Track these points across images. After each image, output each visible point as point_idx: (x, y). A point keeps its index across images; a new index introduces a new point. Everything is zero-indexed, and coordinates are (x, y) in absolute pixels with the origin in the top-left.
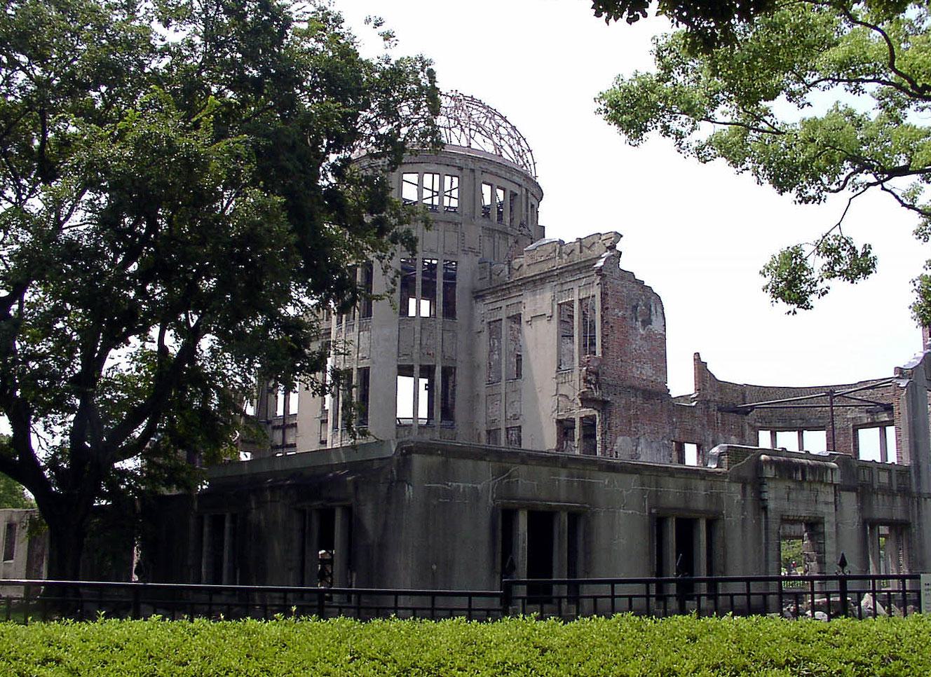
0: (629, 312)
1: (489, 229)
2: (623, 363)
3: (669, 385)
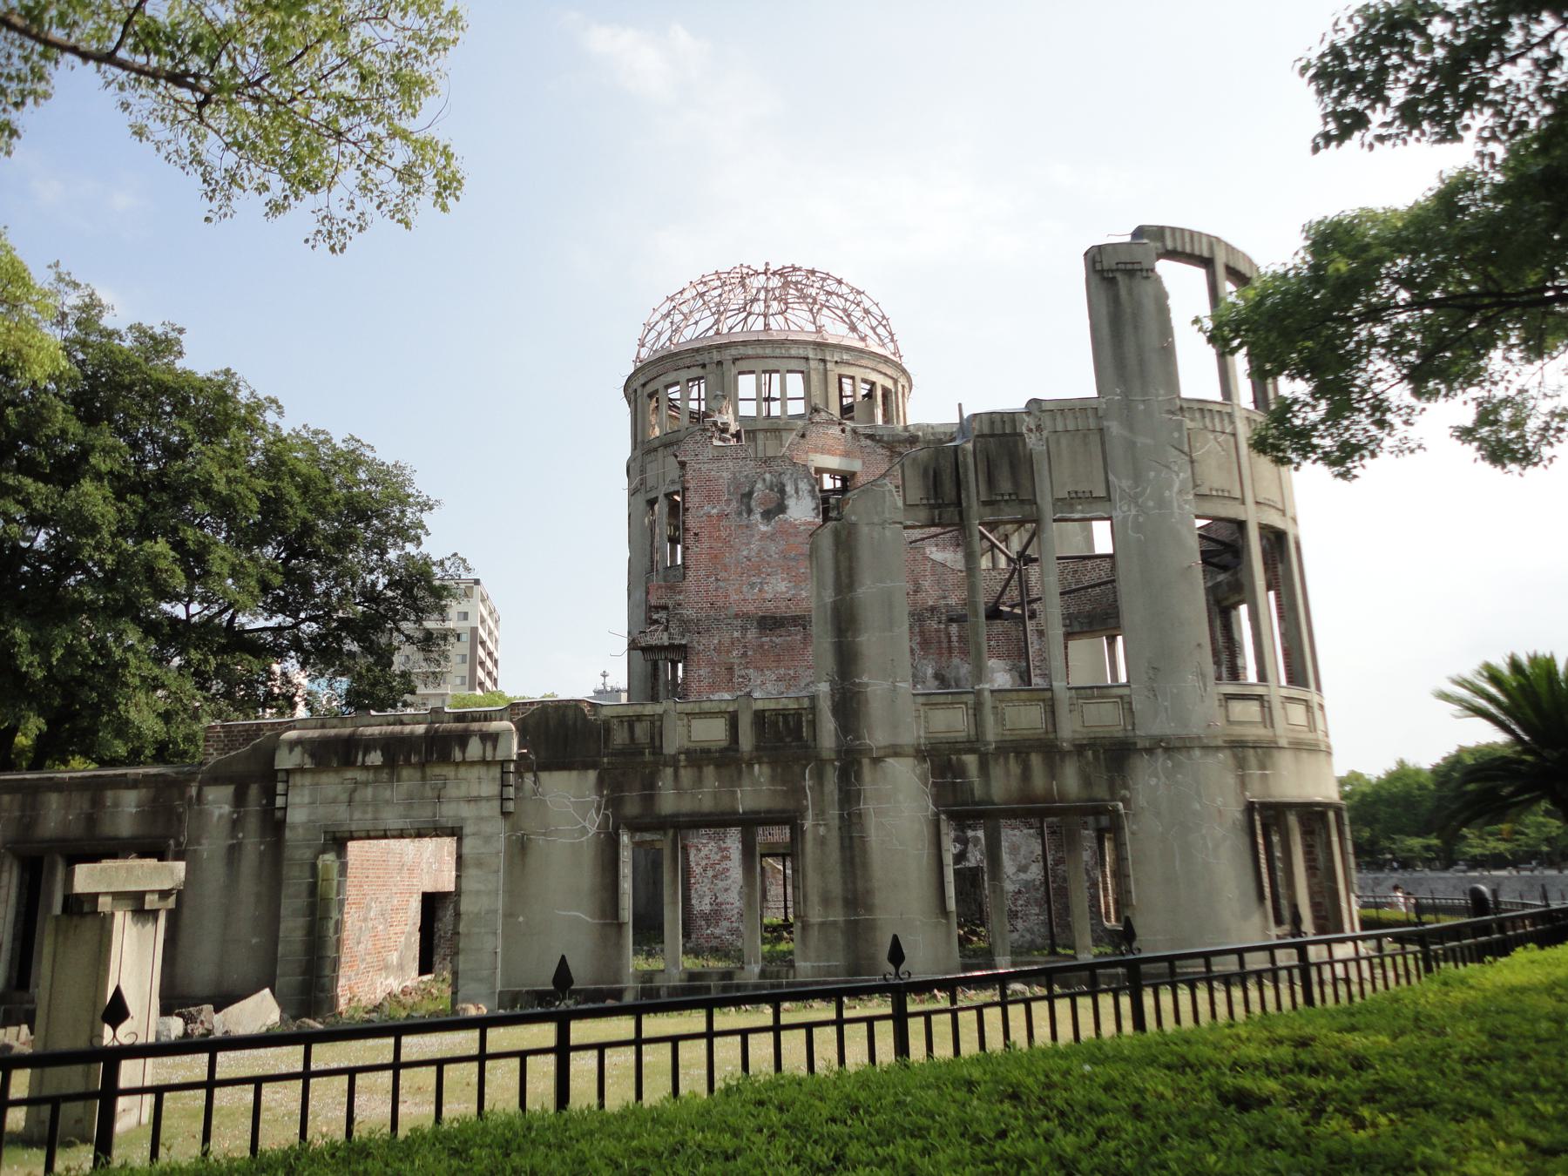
0: (734, 504)
2: (720, 583)
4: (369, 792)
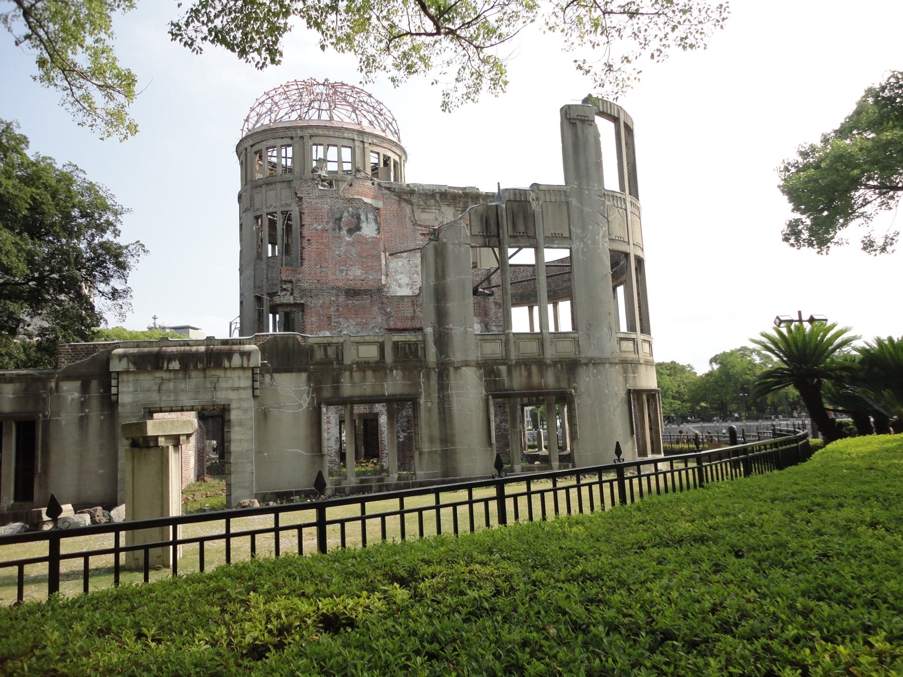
0: (331, 224)
4: (171, 385)
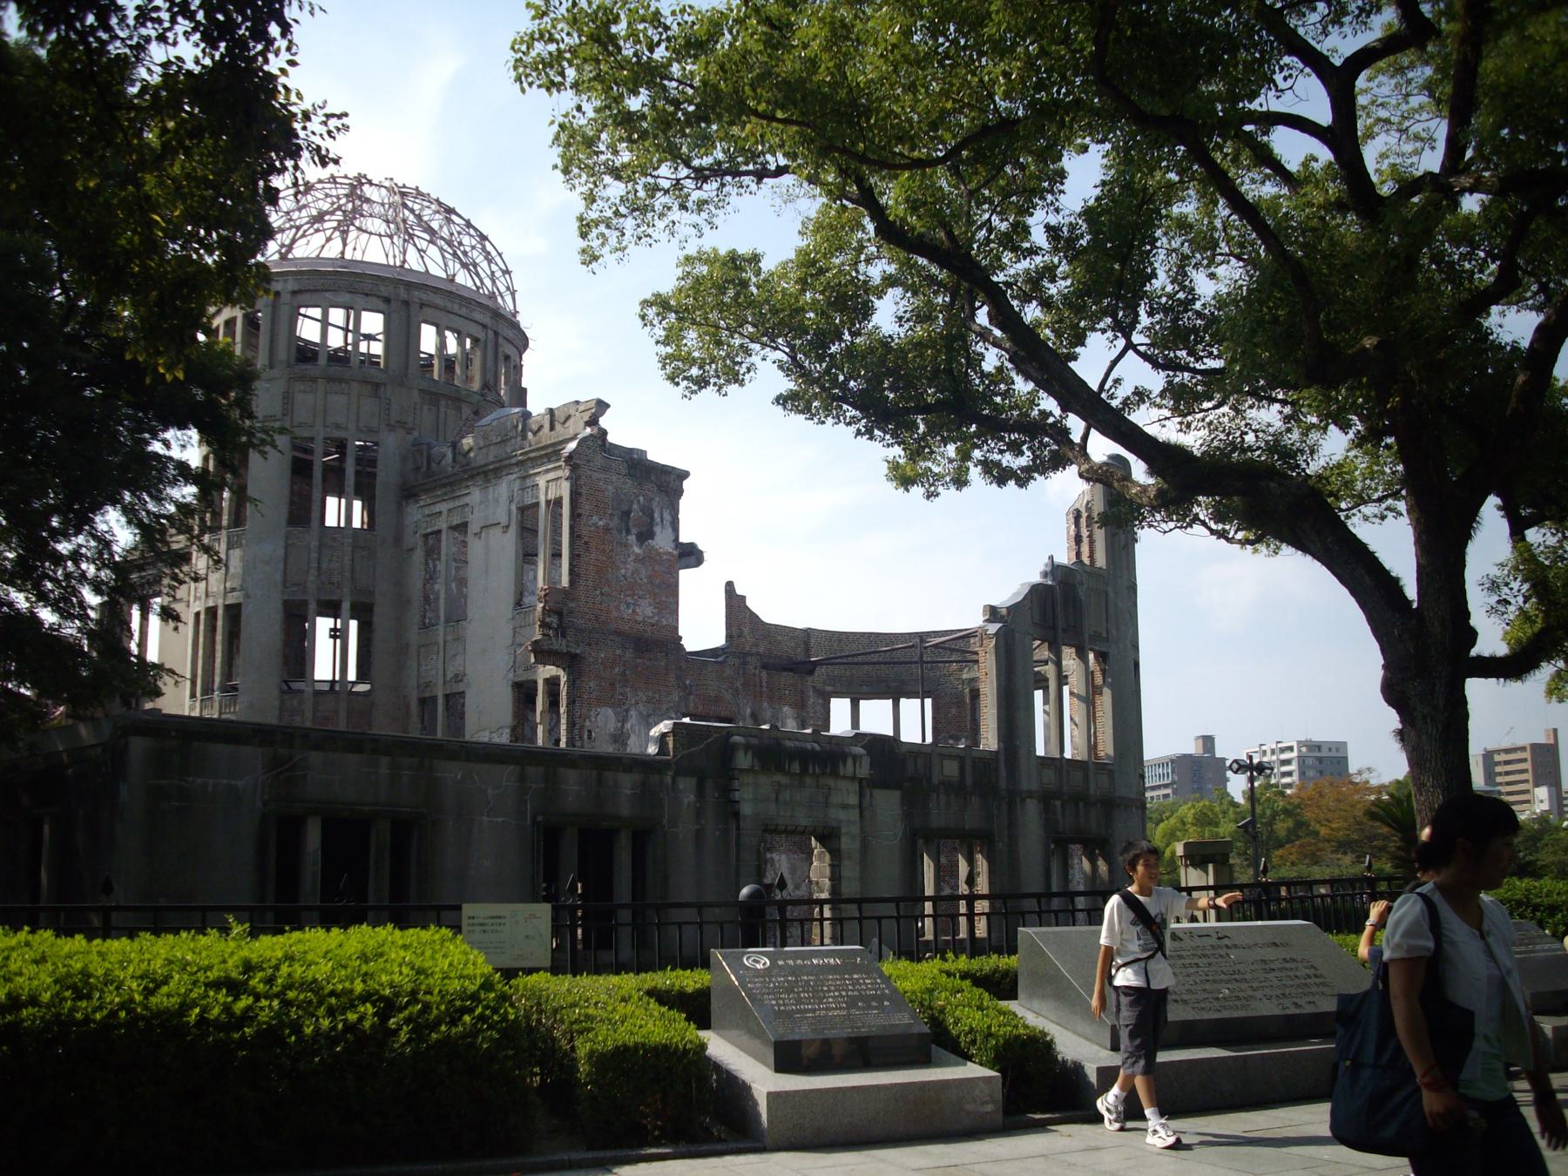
0: (616, 521)
1: (432, 393)
3: (681, 633)
